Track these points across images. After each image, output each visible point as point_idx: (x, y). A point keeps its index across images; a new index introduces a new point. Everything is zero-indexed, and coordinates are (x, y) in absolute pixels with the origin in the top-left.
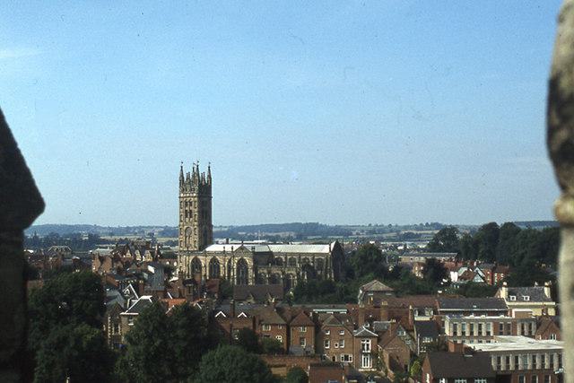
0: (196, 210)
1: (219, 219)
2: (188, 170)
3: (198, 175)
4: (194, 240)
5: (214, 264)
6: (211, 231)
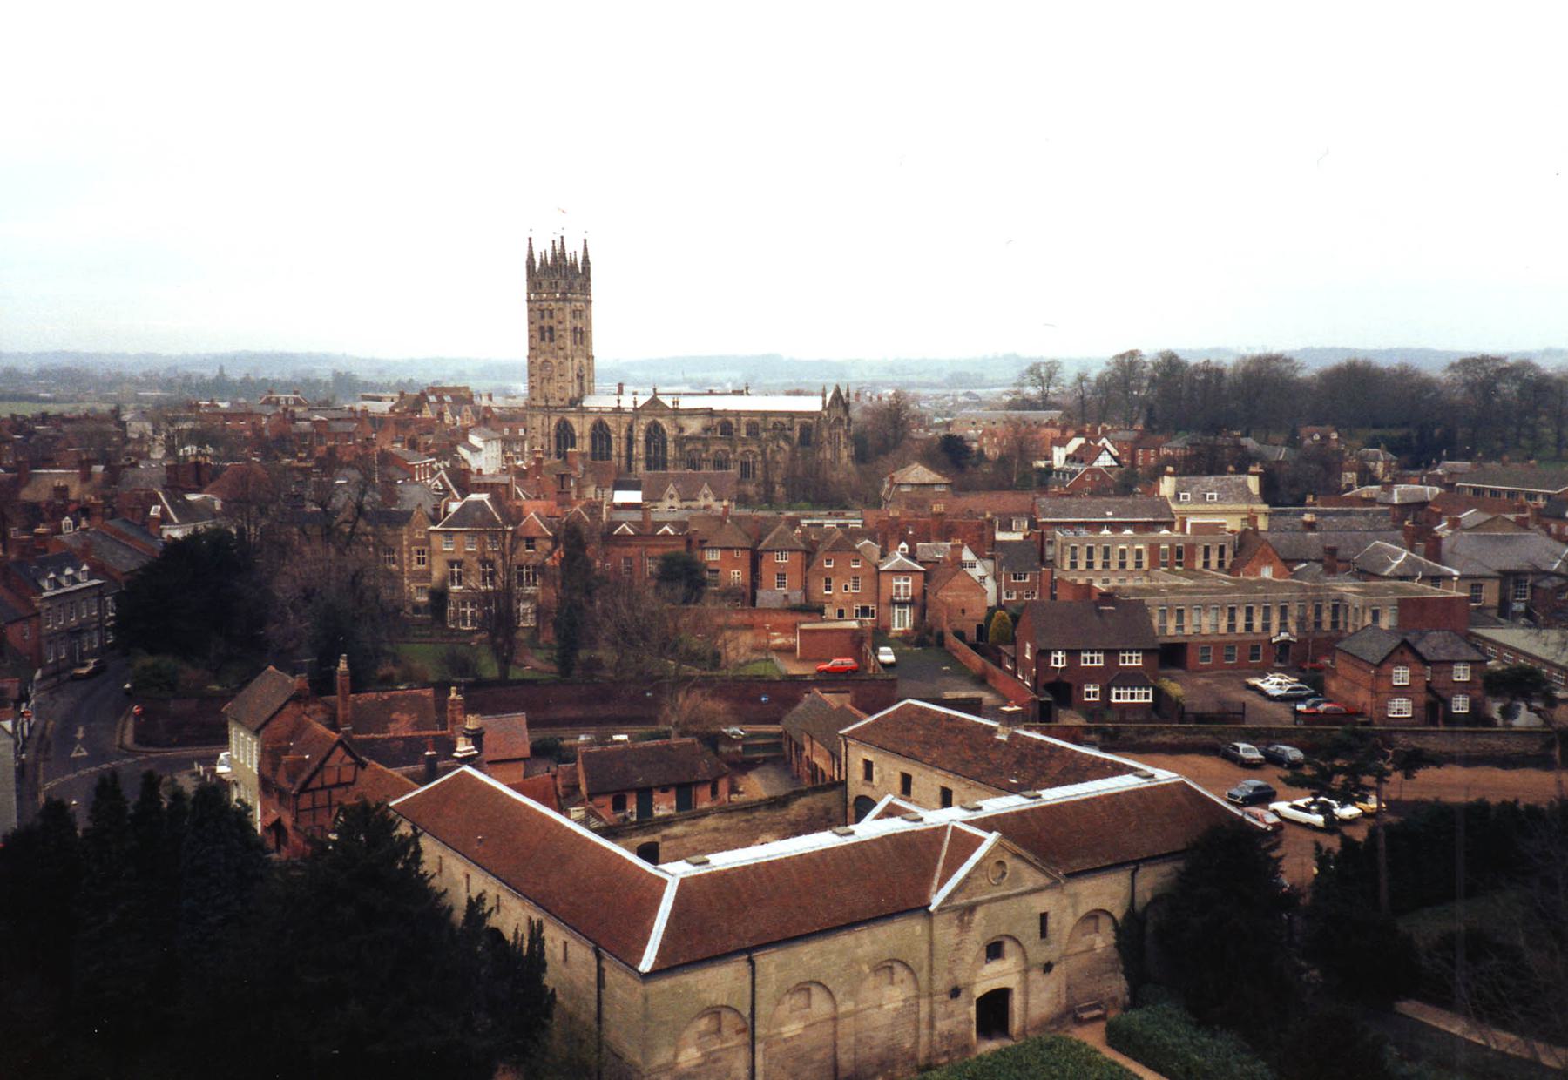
2: (543, 248)
6: (591, 369)
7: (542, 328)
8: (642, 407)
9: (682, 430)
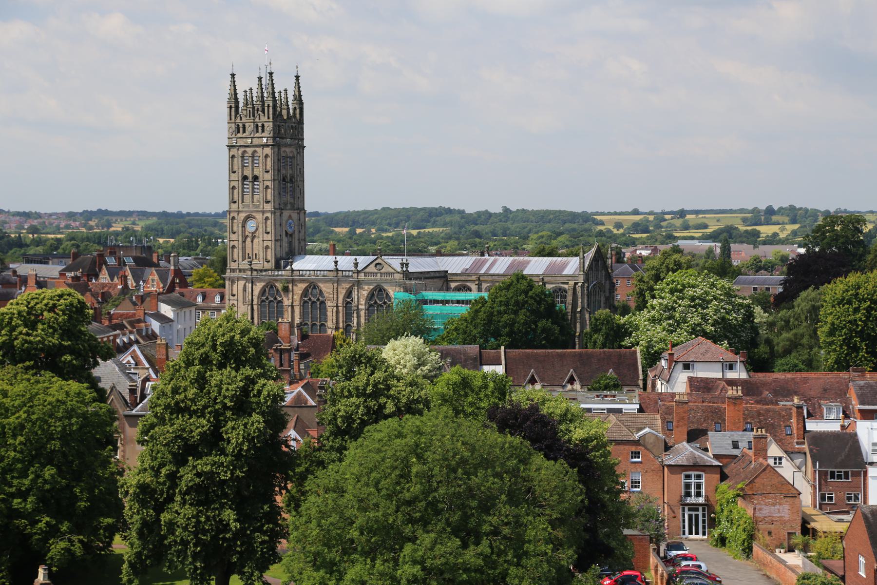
0: (268, 176)
1: (321, 195)
2: (246, 84)
3: (273, 93)
4: (263, 247)
5: (313, 300)
6: (302, 225)
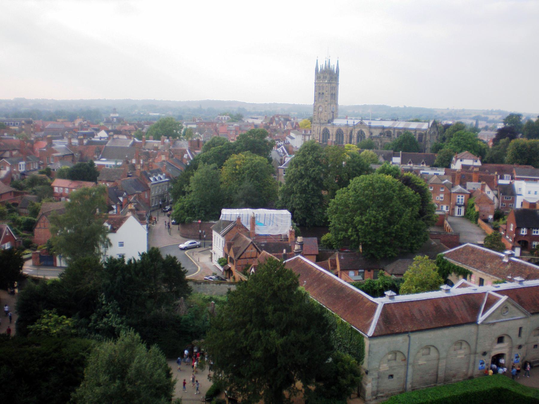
2: (322, 64)
6: (337, 109)
7: (320, 93)
8: (356, 125)
9: (371, 134)
